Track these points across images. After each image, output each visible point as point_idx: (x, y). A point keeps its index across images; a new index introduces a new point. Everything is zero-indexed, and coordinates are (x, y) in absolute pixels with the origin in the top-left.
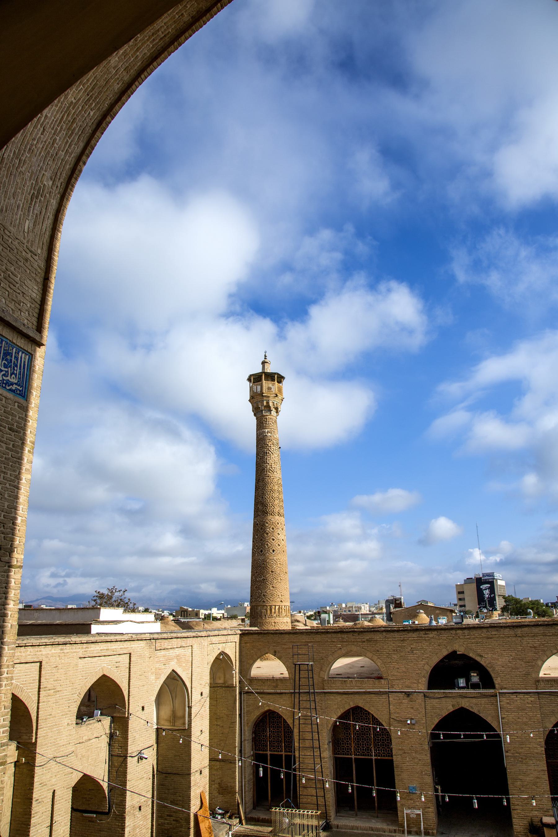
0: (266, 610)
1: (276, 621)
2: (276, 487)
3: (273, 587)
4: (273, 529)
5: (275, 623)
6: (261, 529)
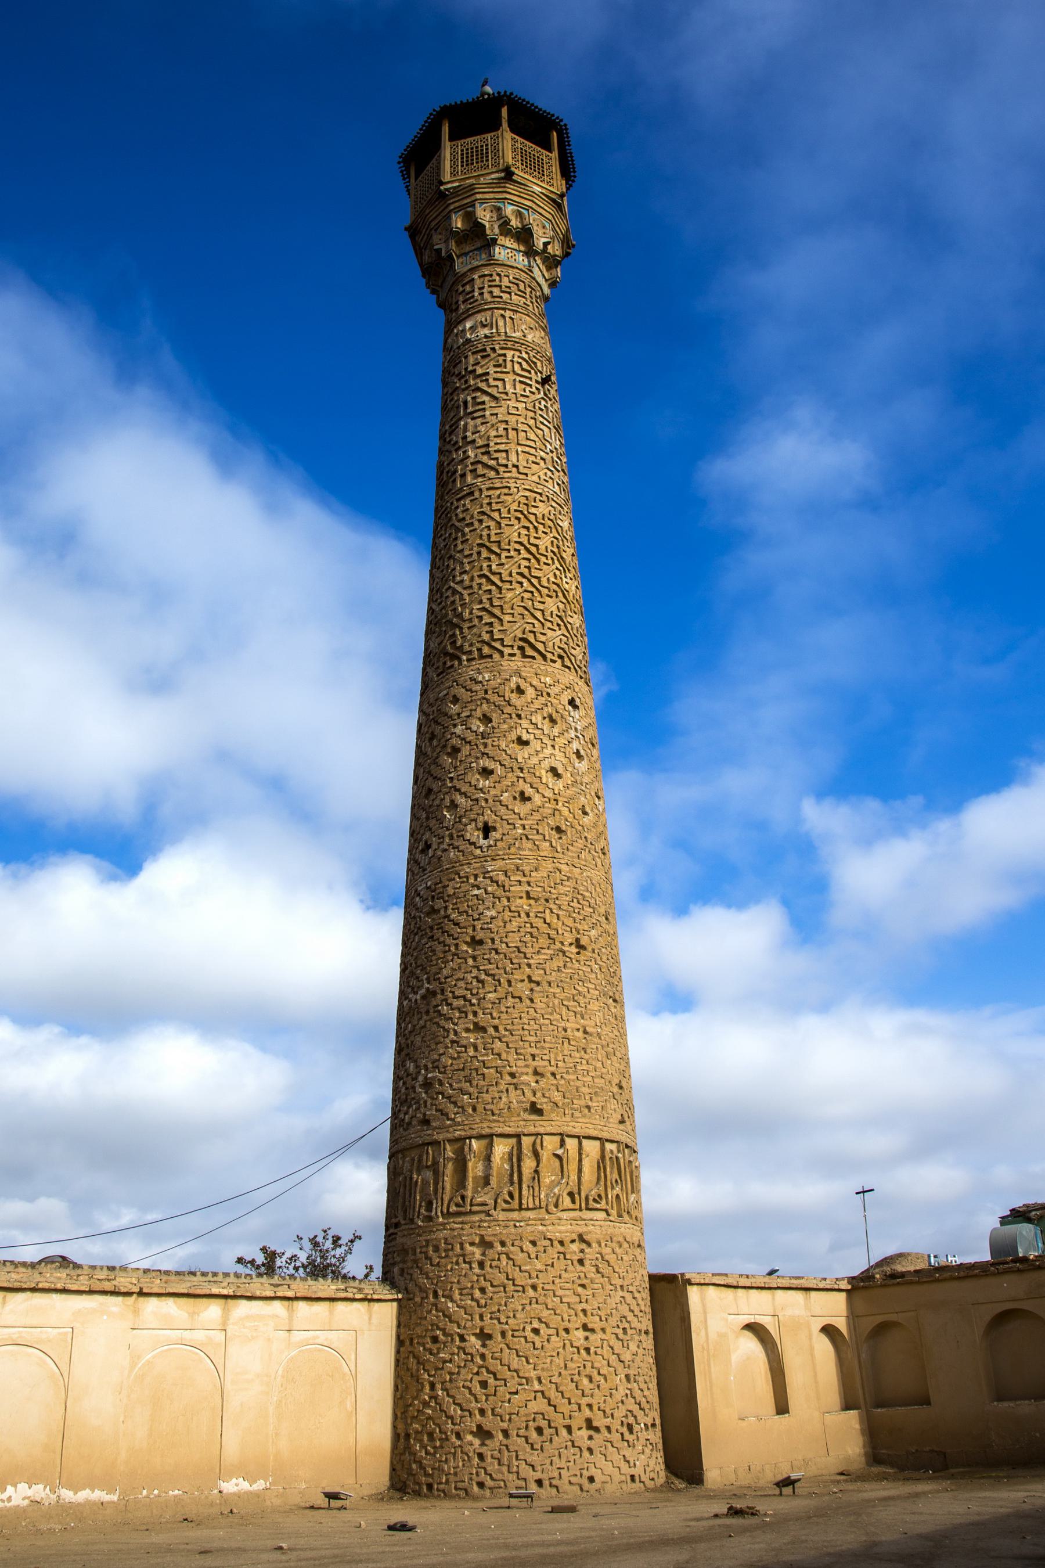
0: (435, 1168)
1: (490, 1232)
2: (513, 533)
3: (479, 1028)
4: (486, 719)
5: (486, 1244)
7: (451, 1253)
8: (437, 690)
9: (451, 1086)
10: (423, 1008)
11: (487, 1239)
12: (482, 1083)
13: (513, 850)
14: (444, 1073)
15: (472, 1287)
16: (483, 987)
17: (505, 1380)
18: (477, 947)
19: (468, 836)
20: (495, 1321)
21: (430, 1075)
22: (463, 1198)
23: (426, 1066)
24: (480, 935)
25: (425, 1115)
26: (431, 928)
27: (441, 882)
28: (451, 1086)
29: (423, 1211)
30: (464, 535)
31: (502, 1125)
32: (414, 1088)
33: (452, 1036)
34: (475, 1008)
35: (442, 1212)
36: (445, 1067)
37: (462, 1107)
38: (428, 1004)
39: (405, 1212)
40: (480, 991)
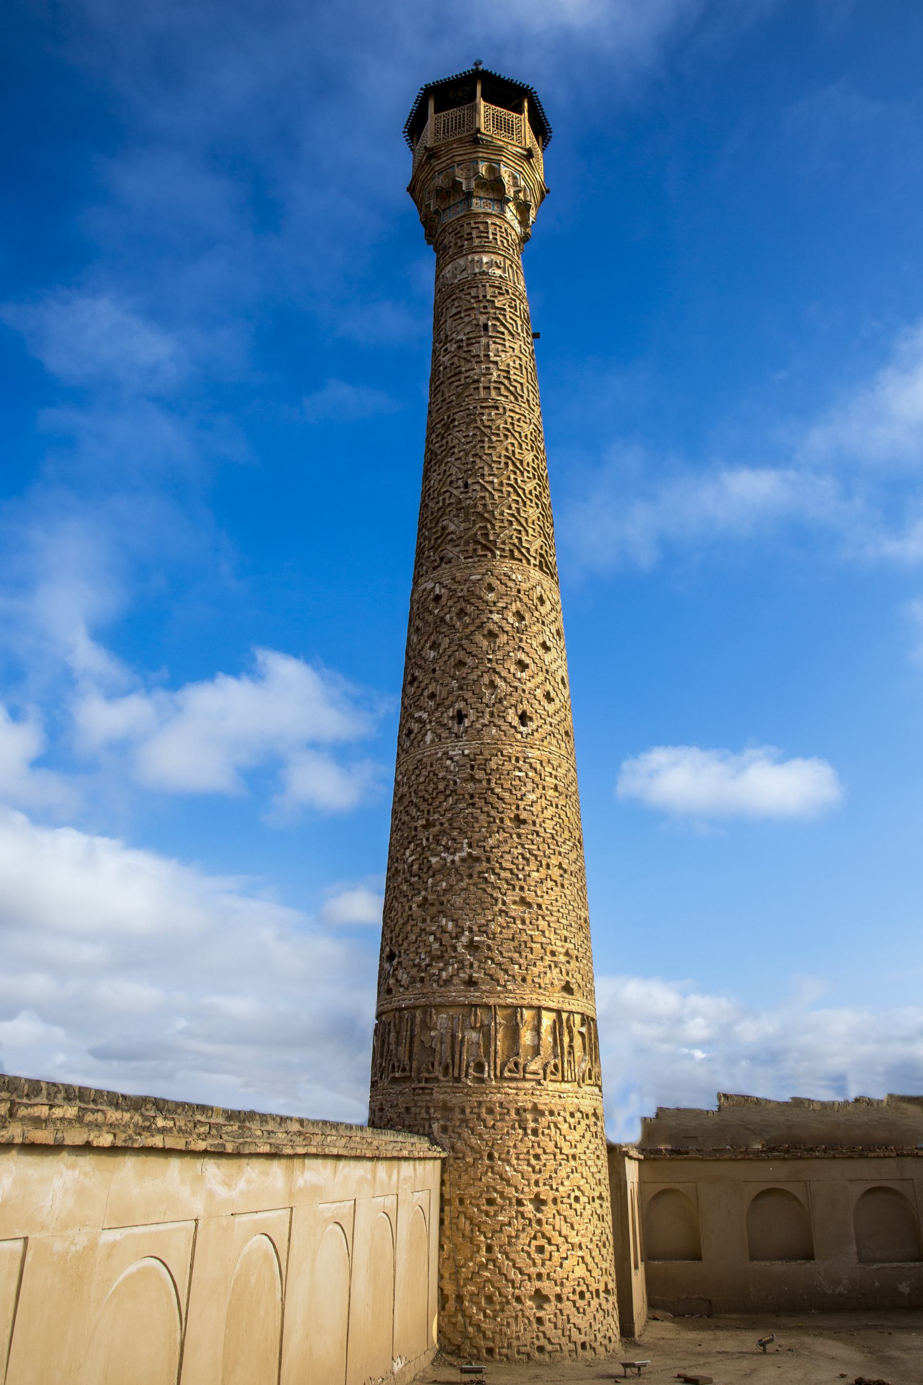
1: (543, 1101)
3: (523, 902)
6: (462, 613)
7: (507, 1117)
8: (467, 571)
9: (501, 953)
10: (464, 870)
11: (541, 1107)
12: (530, 956)
13: (545, 743)
14: (494, 939)
15: (528, 1152)
16: (528, 865)
17: (557, 1245)
18: (522, 826)
19: (509, 719)
20: (548, 1187)
21: (476, 938)
22: (516, 1064)
23: (471, 930)
24: (524, 815)
25: (471, 977)
26: (472, 796)
27: (481, 754)
28: (501, 953)
29: (471, 1071)
30: (490, 441)
31: (547, 999)
32: (455, 949)
33: (500, 905)
34: (522, 883)
35: (495, 1076)
36: (494, 934)
37: (513, 976)
38: (470, 868)
39: (446, 1068)
40: (526, 868)
